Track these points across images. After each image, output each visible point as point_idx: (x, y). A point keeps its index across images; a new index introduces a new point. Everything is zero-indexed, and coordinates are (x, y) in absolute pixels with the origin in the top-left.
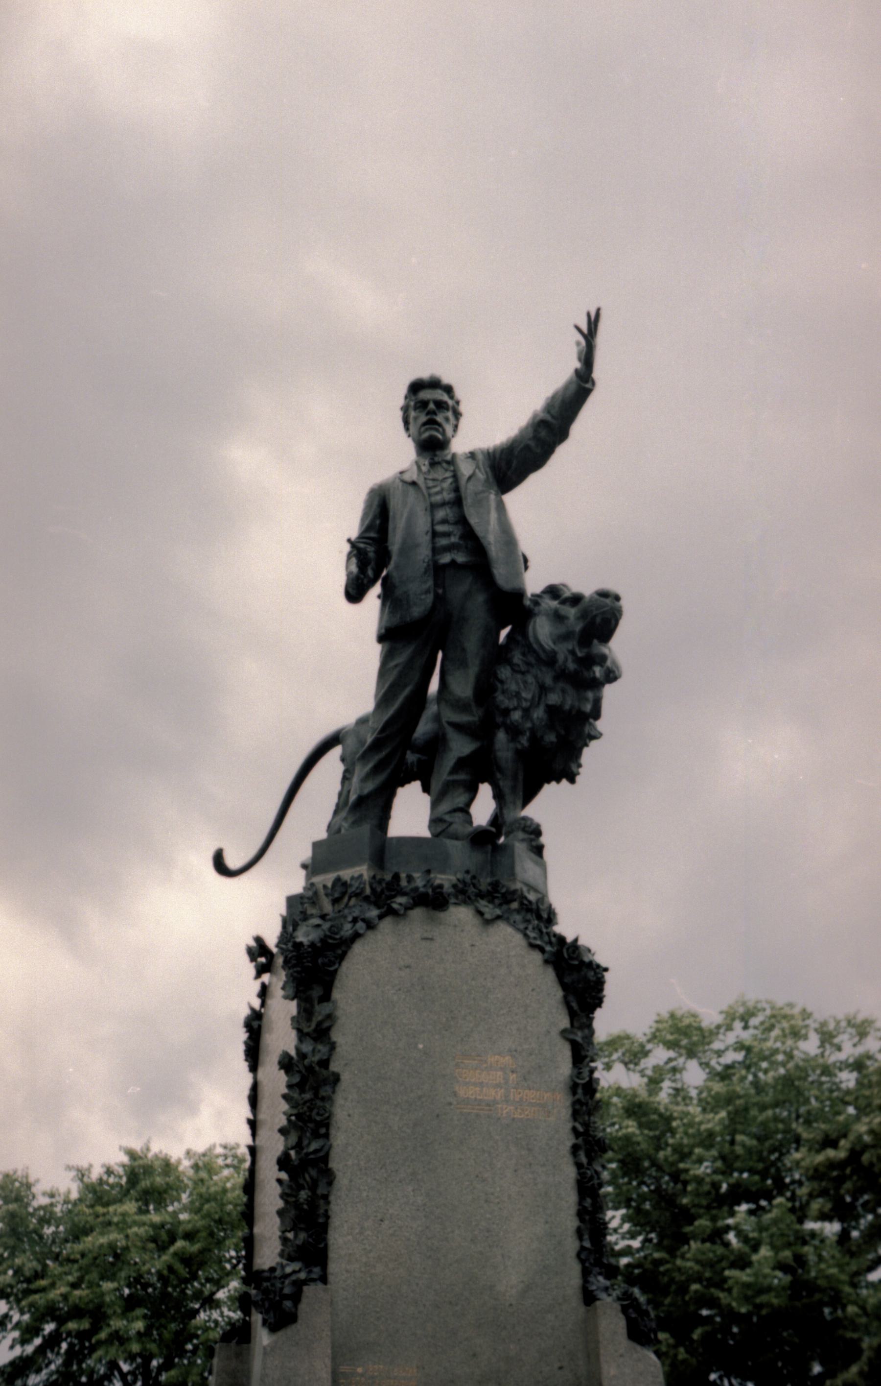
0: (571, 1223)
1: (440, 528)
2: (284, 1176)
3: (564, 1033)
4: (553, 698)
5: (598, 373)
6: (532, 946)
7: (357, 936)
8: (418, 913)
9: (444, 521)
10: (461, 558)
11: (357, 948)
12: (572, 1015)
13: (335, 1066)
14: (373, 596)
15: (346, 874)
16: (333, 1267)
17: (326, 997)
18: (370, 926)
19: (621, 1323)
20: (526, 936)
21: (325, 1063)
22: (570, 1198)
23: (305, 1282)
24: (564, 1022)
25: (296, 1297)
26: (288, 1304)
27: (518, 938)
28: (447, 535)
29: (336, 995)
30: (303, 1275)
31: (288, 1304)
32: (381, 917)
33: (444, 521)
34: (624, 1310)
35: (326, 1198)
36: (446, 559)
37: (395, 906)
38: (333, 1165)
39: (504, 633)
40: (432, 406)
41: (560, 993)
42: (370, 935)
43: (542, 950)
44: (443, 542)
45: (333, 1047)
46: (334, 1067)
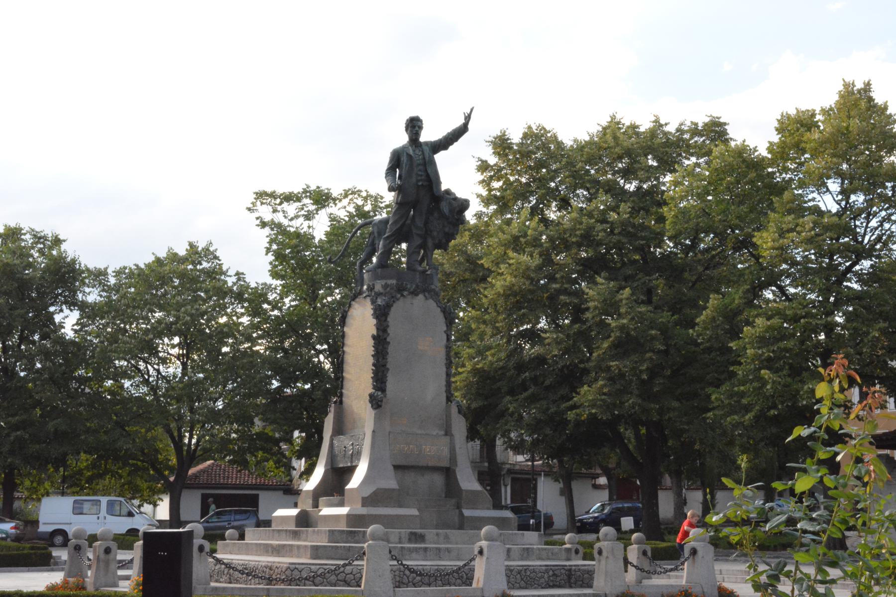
1: (420, 173)
2: (374, 368)
4: (447, 230)
5: (469, 126)
7: (394, 302)
8: (410, 297)
9: (420, 170)
10: (425, 183)
11: (395, 305)
12: (447, 326)
13: (388, 340)
15: (390, 282)
17: (386, 320)
18: (398, 299)
19: (457, 410)
21: (385, 339)
24: (445, 329)
25: (381, 401)
27: (435, 304)
28: (421, 175)
29: (389, 319)
31: (379, 403)
33: (420, 170)
36: (420, 183)
42: (397, 302)
44: (419, 178)
45: (389, 334)
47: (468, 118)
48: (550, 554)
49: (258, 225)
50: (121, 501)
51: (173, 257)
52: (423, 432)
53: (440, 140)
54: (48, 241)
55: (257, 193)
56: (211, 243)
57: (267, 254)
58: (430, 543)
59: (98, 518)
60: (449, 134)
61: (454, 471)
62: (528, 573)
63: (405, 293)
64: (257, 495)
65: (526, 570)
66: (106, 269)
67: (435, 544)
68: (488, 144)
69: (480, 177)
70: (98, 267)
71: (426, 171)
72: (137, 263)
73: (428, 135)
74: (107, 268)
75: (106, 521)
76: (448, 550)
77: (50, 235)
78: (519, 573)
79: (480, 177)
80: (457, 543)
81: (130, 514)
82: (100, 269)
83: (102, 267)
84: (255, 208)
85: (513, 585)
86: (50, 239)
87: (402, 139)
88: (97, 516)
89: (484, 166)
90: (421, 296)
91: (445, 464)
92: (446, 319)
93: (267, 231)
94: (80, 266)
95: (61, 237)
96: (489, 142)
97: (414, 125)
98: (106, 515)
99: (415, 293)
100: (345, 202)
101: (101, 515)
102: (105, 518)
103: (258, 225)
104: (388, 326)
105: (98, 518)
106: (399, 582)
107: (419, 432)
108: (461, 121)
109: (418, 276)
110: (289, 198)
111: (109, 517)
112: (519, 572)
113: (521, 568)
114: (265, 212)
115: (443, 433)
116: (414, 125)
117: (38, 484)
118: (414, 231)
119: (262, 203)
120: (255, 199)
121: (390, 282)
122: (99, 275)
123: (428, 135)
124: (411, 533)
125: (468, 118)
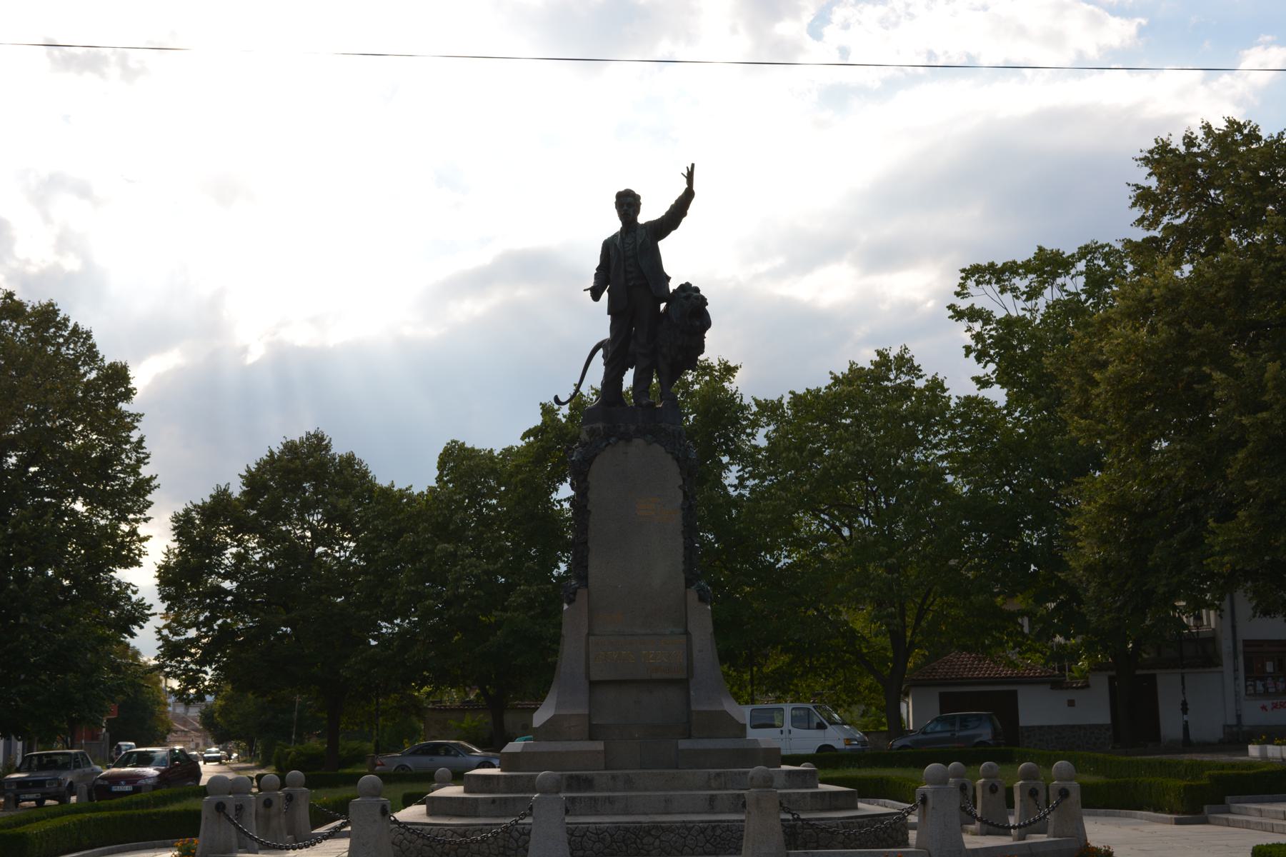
0: (681, 559)
3: (680, 487)
5: (695, 188)
6: (668, 452)
7: (596, 455)
11: (597, 459)
14: (605, 296)
15: (595, 426)
16: (591, 581)
17: (585, 480)
19: (696, 597)
20: (666, 449)
21: (586, 506)
22: (681, 550)
23: (579, 588)
24: (681, 483)
25: (575, 594)
26: (571, 596)
30: (577, 586)
32: (606, 446)
34: (698, 591)
35: (587, 556)
36: (631, 284)
37: (611, 441)
38: (589, 545)
39: (663, 306)
40: (625, 208)
41: (679, 470)
43: (672, 453)
46: (589, 508)
49: (951, 317)
50: (809, 709)
51: (856, 373)
53: (663, 217)
54: (716, 371)
55: (963, 271)
56: (906, 349)
57: (967, 356)
58: (602, 790)
59: (782, 732)
60: (672, 206)
62: (718, 832)
63: (613, 440)
64: (1015, 693)
65: (714, 828)
66: (780, 401)
67: (610, 790)
68: (1139, 162)
69: (1138, 213)
70: (769, 398)
72: (792, 389)
73: (649, 213)
74: (782, 398)
75: (791, 736)
76: (610, 800)
77: (716, 363)
78: (703, 832)
79: (1138, 213)
80: (646, 789)
81: (821, 726)
82: (773, 401)
83: (775, 398)
84: (965, 291)
85: (692, 849)
86: (717, 368)
87: (614, 225)
88: (779, 729)
89: (1144, 197)
90: (638, 442)
92: (681, 469)
93: (964, 324)
94: (741, 400)
95: (732, 364)
96: (1141, 159)
97: (627, 203)
98: (791, 728)
99: (627, 438)
100: (1081, 266)
101: (785, 729)
102: (790, 731)
103: (951, 317)
104: (587, 488)
105: (782, 732)
106: (504, 846)
108: (683, 186)
110: (1012, 268)
111: (794, 730)
112: (703, 831)
113: (706, 825)
114: (985, 297)
116: (627, 203)
117: (740, 689)
119: (978, 283)
120: (962, 278)
121: (595, 426)
122: (769, 409)
123: (649, 213)
124: (571, 777)
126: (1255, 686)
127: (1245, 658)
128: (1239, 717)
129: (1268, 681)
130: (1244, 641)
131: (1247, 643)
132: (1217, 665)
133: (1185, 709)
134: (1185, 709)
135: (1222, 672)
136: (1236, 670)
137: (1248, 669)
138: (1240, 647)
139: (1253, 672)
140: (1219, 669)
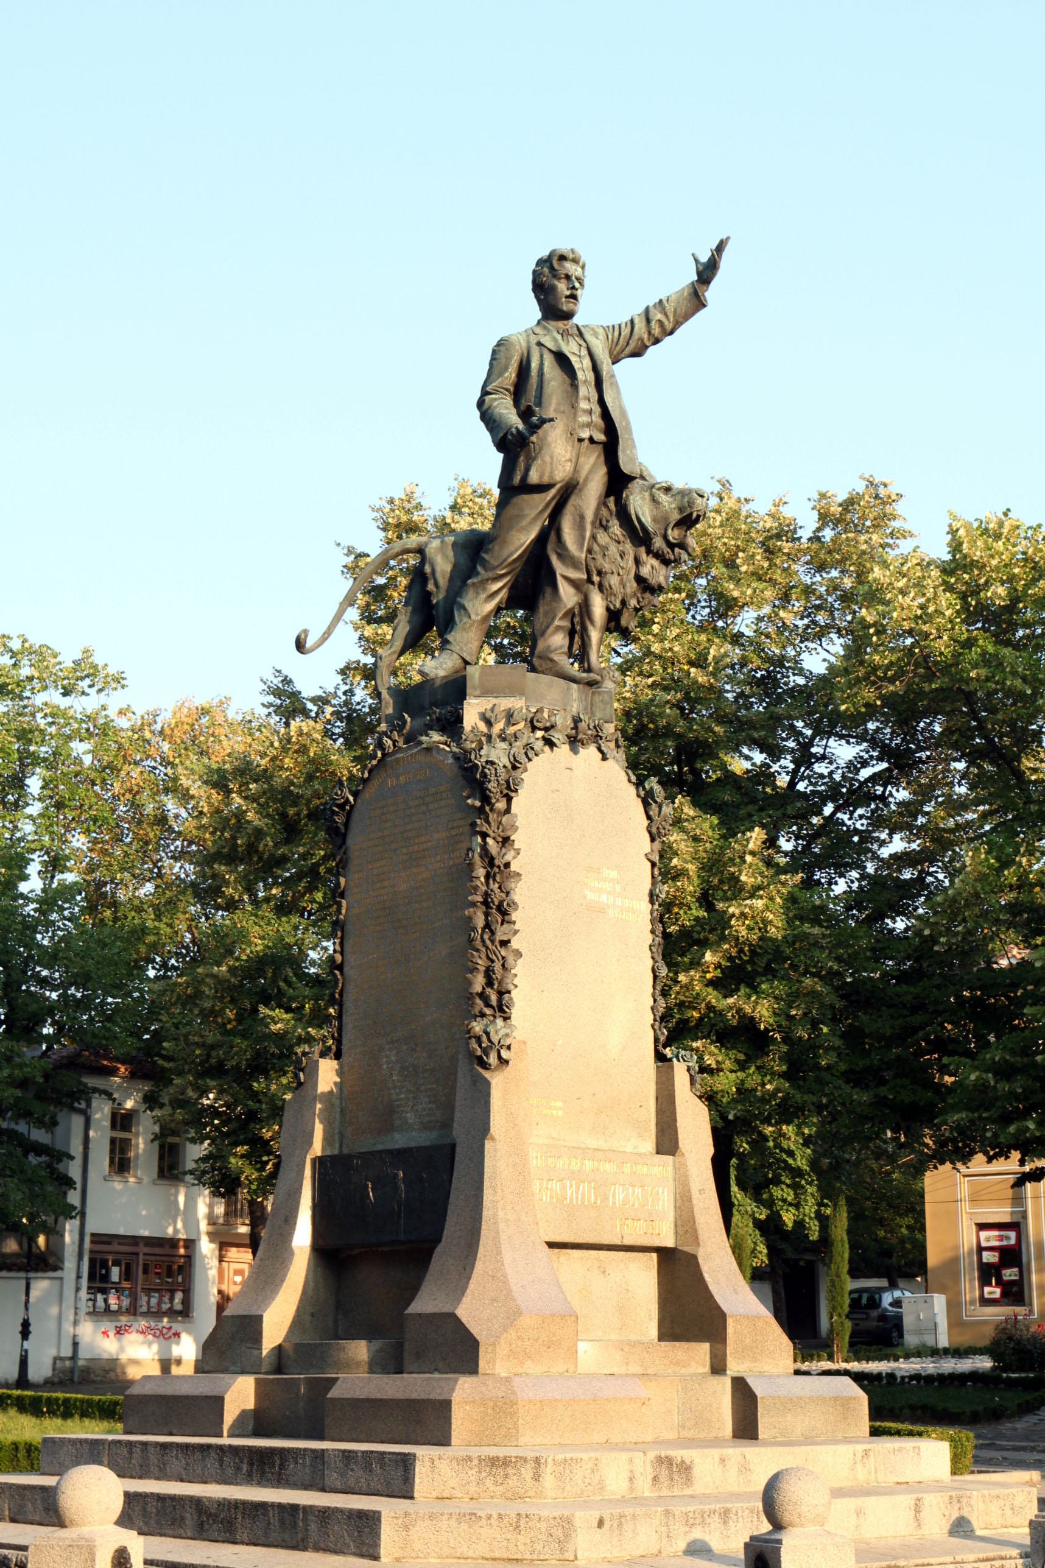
21: (507, 865)
31: (504, 1054)
47: (707, 272)
48: (1008, 1512)
52: (601, 1143)
61: (693, 1259)
71: (601, 402)
91: (668, 1241)
104: (515, 829)
107: (592, 1143)
109: (575, 695)
115: (650, 1145)
118: (559, 568)
125: (707, 272)
126: (95, 1300)
127: (92, 1262)
128: (75, 1345)
129: (111, 1296)
130: (93, 1235)
131: (97, 1238)
132: (56, 1268)
133: (25, 1333)
134: (25, 1333)
135: (61, 1279)
136: (79, 1277)
137: (92, 1277)
138: (87, 1239)
139: (99, 1281)
140: (58, 1274)
